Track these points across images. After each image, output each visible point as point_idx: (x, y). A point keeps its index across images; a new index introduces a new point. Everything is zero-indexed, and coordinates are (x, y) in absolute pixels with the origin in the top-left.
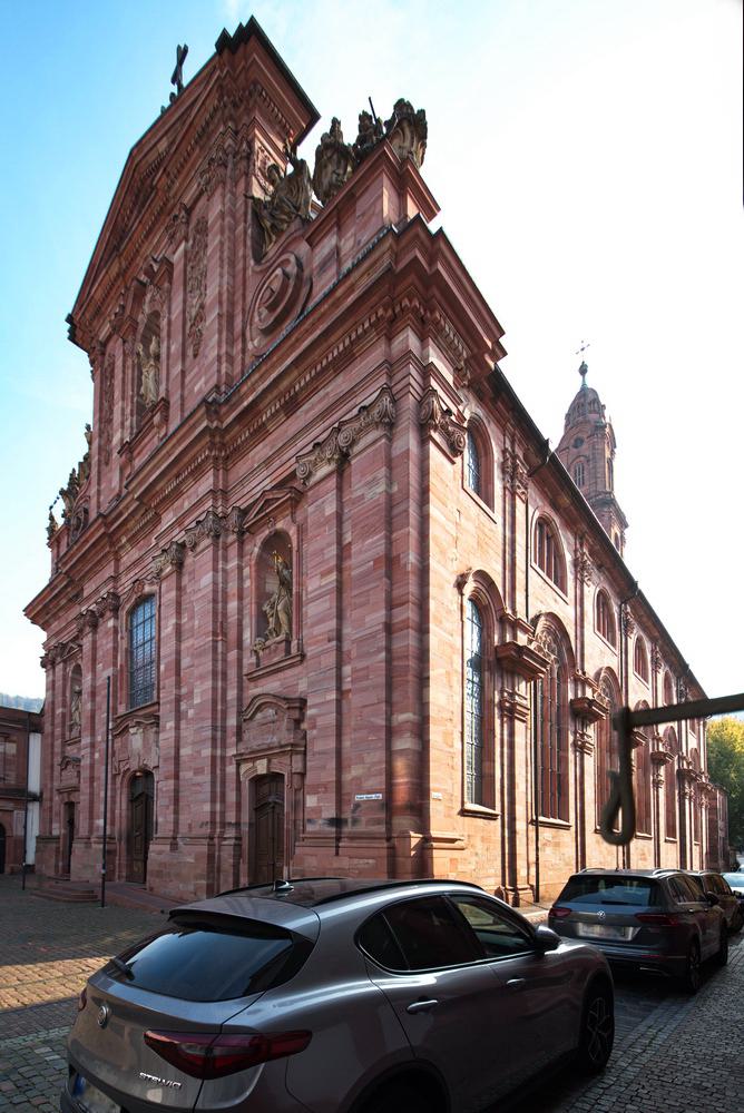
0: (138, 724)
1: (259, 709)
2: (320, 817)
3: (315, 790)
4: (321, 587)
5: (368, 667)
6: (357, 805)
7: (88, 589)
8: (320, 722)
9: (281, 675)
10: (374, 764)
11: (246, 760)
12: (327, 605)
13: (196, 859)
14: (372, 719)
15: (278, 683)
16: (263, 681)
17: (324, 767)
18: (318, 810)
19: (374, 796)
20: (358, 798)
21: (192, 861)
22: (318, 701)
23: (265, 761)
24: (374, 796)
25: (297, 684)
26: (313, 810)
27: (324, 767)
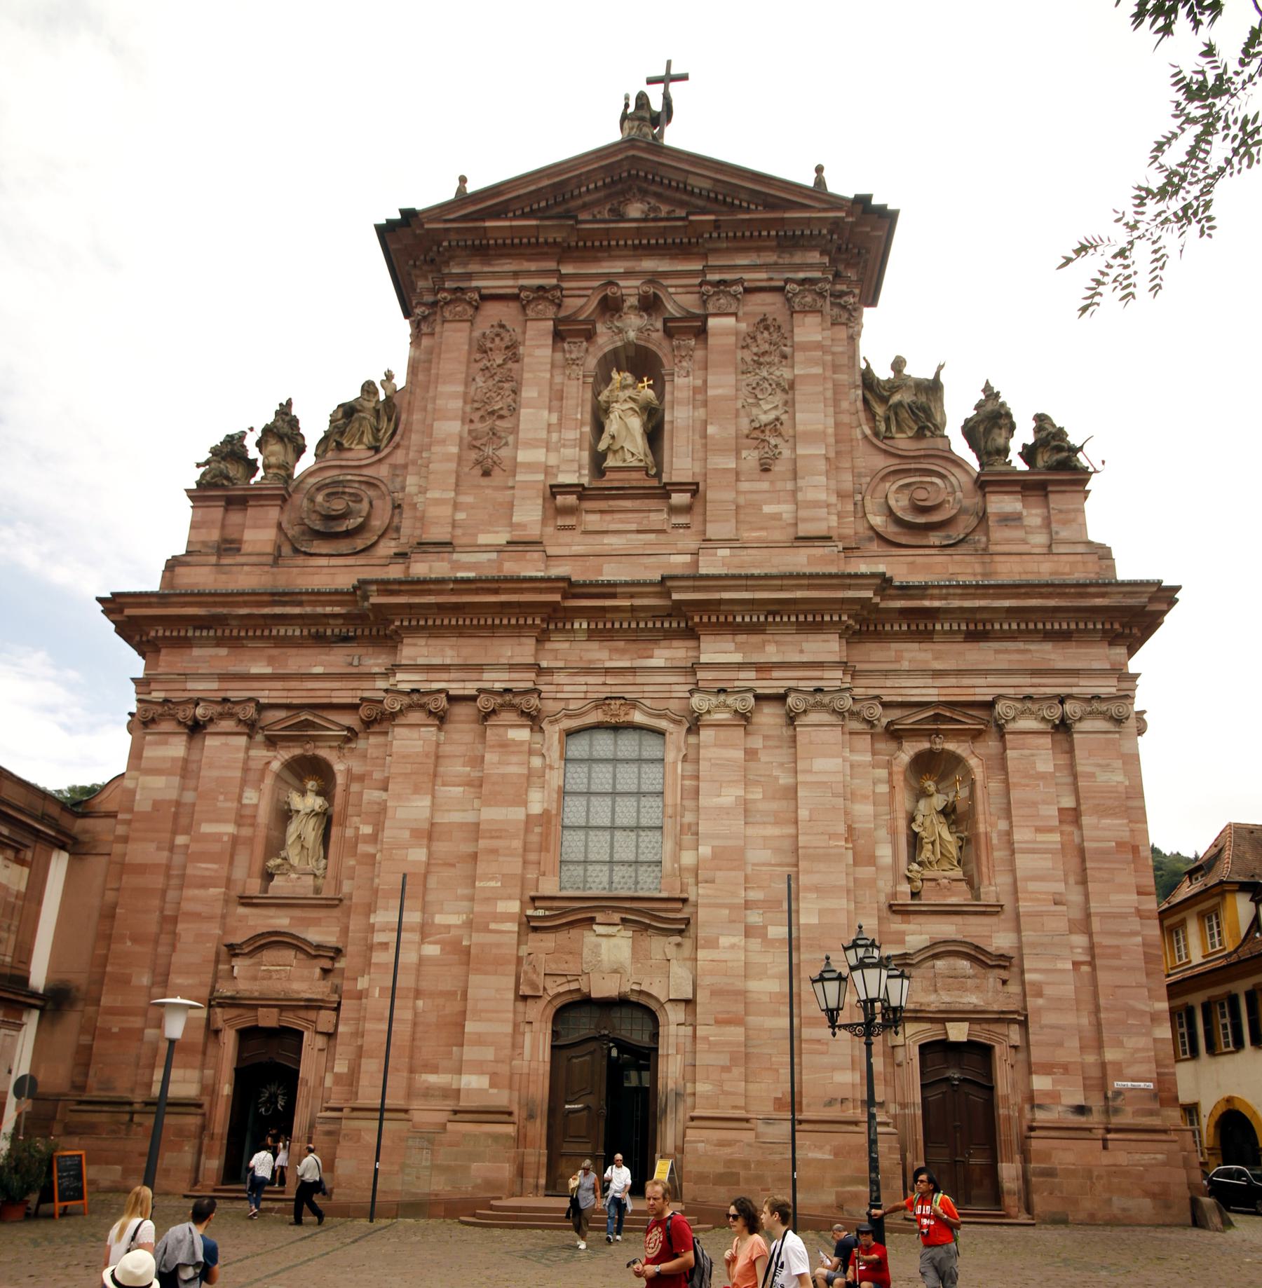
0: (624, 920)
1: (936, 956)
2: (1059, 1104)
3: (1047, 1069)
4: (1035, 842)
5: (1118, 947)
6: (1118, 1093)
7: (415, 650)
8: (1048, 991)
9: (958, 919)
10: (1137, 1050)
11: (917, 1020)
12: (1049, 864)
13: (836, 1155)
14: (1132, 1002)
15: (954, 928)
16: (921, 919)
17: (1060, 1045)
18: (1054, 1096)
19: (1142, 1085)
20: (1118, 1084)
21: (832, 1157)
22: (1042, 965)
23: (966, 1025)
24: (1142, 1085)
25: (991, 937)
26: (1047, 1094)
27: (1060, 1045)
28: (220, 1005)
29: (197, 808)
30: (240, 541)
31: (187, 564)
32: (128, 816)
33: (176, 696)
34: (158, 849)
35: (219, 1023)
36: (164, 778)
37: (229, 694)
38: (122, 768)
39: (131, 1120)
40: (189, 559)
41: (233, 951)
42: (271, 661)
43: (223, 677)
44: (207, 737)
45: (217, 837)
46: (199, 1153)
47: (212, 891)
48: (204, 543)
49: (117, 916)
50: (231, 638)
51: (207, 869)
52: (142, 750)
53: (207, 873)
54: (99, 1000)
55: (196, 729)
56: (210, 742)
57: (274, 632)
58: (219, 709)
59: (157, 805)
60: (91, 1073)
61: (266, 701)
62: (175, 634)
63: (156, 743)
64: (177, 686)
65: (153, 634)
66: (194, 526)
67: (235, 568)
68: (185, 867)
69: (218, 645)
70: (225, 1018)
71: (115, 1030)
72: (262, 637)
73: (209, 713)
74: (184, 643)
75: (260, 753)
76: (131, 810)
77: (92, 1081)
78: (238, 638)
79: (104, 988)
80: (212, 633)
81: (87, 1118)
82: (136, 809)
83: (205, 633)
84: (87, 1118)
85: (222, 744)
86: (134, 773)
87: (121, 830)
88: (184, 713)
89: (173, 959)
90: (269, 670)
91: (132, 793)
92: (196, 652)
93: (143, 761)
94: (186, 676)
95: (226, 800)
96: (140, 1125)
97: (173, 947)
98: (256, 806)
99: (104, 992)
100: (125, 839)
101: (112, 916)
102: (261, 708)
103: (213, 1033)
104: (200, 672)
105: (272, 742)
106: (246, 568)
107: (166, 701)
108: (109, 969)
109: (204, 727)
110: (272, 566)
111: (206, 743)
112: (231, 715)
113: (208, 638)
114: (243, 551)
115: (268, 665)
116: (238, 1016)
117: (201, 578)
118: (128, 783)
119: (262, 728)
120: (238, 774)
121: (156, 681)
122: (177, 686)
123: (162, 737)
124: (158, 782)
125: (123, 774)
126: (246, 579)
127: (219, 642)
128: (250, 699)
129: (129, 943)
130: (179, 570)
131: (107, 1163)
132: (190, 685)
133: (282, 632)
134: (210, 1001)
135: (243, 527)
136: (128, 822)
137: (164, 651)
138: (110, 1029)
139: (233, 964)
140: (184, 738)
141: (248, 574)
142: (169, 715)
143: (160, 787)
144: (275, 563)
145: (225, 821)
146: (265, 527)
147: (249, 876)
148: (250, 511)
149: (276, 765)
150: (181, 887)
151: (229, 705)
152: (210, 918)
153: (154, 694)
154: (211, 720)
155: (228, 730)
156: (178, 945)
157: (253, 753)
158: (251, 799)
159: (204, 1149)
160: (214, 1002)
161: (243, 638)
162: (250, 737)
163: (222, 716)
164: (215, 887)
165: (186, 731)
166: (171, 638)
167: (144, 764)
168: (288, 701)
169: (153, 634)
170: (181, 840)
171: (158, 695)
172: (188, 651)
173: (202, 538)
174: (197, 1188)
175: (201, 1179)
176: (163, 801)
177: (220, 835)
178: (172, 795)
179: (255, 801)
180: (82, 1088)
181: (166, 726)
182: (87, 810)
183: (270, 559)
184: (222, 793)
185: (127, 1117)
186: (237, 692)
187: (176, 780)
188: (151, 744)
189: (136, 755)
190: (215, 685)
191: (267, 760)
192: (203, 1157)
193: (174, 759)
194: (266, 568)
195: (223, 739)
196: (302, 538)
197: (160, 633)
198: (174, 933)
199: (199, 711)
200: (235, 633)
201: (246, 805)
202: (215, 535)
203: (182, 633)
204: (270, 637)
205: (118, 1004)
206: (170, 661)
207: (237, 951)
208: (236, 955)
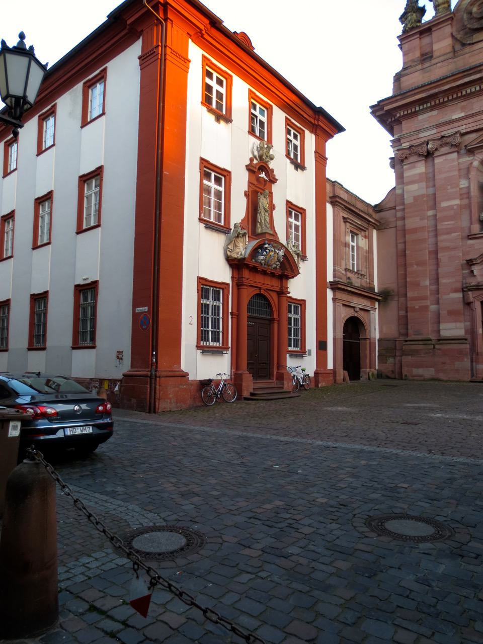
28: (470, 290)
29: (437, 195)
30: (432, 52)
31: (407, 75)
32: (401, 207)
33: (415, 143)
34: (421, 219)
35: (471, 299)
36: (416, 185)
37: (443, 133)
38: (393, 184)
39: (434, 348)
40: (406, 72)
41: (470, 263)
42: (463, 109)
43: (438, 126)
44: (435, 159)
45: (450, 208)
46: (472, 361)
47: (454, 235)
48: (413, 61)
49: (407, 255)
50: (440, 104)
51: (448, 224)
52: (402, 174)
53: (448, 227)
54: (406, 294)
55: (429, 155)
56: (437, 161)
57: (464, 93)
58: (439, 143)
59: (416, 198)
60: (409, 327)
61: (464, 131)
62: (409, 111)
63: (410, 169)
64: (415, 137)
65: (398, 115)
66: (404, 55)
67: (432, 67)
68: (436, 226)
69: (432, 110)
70: (474, 296)
71: (417, 307)
72: (457, 98)
73: (435, 147)
74: (415, 114)
75: (466, 159)
76: (403, 204)
77: (410, 331)
78: (444, 102)
79: (408, 289)
80: (429, 105)
81: (413, 347)
82: (405, 203)
83: (425, 106)
84: (413, 347)
85: (444, 160)
86: (400, 186)
87: (399, 214)
88: (423, 150)
89: (439, 271)
90: (463, 115)
91: (403, 195)
92: (420, 117)
93: (405, 179)
94: (418, 131)
95: (452, 188)
96: (439, 349)
97: (438, 265)
98: (469, 187)
99: (408, 291)
100: (403, 218)
101: (405, 255)
102: (462, 135)
103: (468, 304)
104: (425, 127)
105: (471, 151)
106: (438, 65)
107: (411, 146)
108: (408, 280)
109: (433, 154)
110: (453, 58)
111: (435, 162)
112: (447, 144)
113: (427, 108)
114: (434, 57)
115: (462, 112)
116: (481, 294)
117: (416, 79)
118: (398, 192)
119: (466, 146)
120: (456, 173)
121: (403, 138)
122: (415, 137)
123: (413, 164)
124: (414, 187)
125: (395, 187)
126: (439, 70)
127: (432, 108)
128: (457, 133)
129: (415, 267)
130: (403, 79)
131: (426, 367)
132: (421, 135)
133: (469, 91)
134: (463, 289)
135: (431, 44)
136: (404, 210)
137: (403, 123)
138: (414, 307)
139: (472, 269)
140: (423, 162)
141: (440, 67)
142: (414, 153)
143: (414, 190)
144: (454, 57)
145: (454, 198)
146: (445, 39)
147: (471, 224)
148: (434, 34)
149: (476, 163)
150: (436, 236)
151: (445, 139)
152: (455, 248)
153: (403, 145)
154: (436, 149)
155: (446, 152)
156: (441, 264)
157: (461, 160)
158: (464, 184)
159: (474, 359)
160: (465, 290)
161: (446, 102)
162: (458, 152)
163: (442, 146)
164: (455, 233)
165: (424, 158)
166: (408, 114)
167: (405, 180)
168: (477, 127)
169: (398, 115)
170: (430, 213)
171: (406, 145)
172: (415, 119)
173: (410, 59)
174: (474, 378)
175: (475, 374)
176: (419, 196)
177: (452, 206)
178: (424, 192)
179: (467, 185)
180: (407, 335)
181: (412, 159)
182: (380, 209)
183: (451, 55)
184: (448, 185)
185: (432, 346)
186: (448, 131)
187: (424, 184)
188: (406, 170)
189: (400, 178)
190: (434, 131)
191: (469, 162)
192: (474, 364)
193: (420, 174)
194: (450, 61)
195: (444, 157)
196: (466, 37)
197: (402, 114)
198: (437, 259)
199: (430, 146)
200: (442, 100)
201: (462, 188)
202: (417, 54)
203: (413, 110)
204: (462, 96)
205: (416, 295)
206: (407, 126)
207: (474, 262)
208: (474, 264)
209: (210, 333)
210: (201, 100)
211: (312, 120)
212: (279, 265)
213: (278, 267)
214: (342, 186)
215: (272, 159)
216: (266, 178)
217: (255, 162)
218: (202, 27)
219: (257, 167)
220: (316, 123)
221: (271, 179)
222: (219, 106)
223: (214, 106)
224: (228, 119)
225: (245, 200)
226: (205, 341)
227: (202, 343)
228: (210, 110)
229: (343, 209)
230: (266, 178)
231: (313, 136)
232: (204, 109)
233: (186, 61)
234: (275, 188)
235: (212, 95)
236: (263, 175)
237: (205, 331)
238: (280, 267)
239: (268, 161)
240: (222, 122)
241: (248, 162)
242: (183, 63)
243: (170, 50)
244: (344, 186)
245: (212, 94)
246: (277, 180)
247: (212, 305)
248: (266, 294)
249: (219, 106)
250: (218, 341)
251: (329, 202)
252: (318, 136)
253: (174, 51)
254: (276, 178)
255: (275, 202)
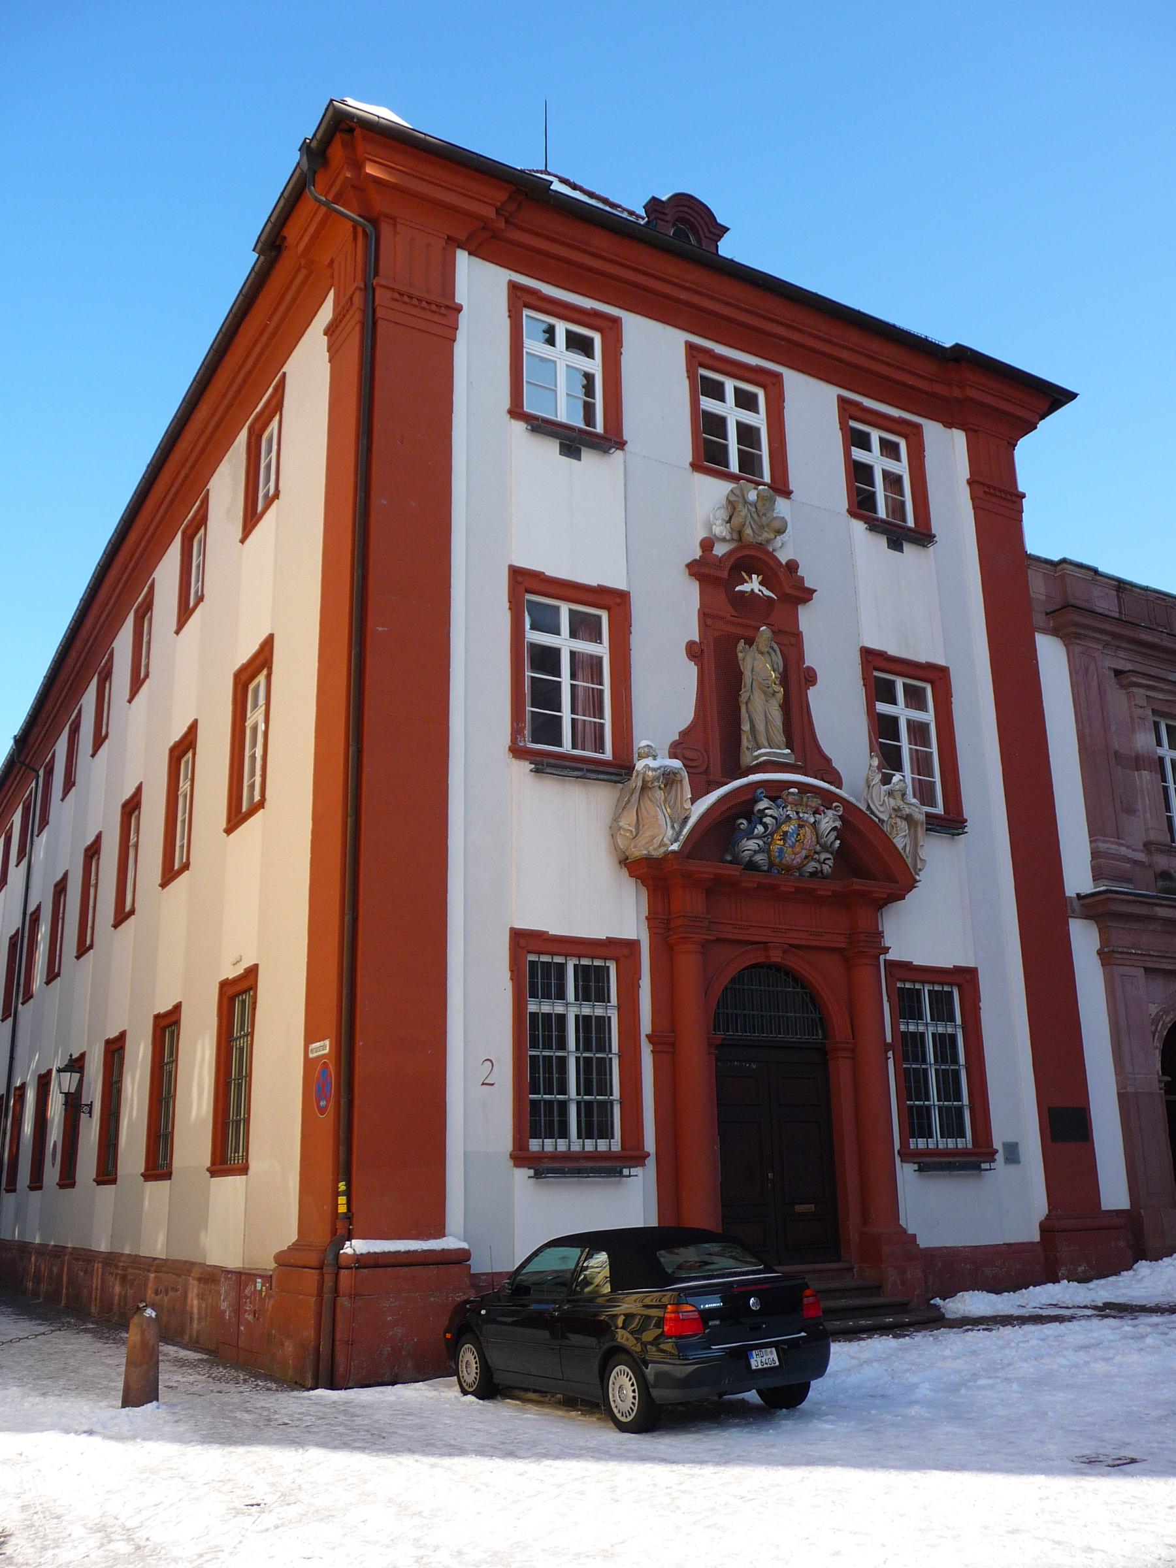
209: (573, 1110)
210: (690, 459)
211: (939, 389)
212: (830, 863)
213: (826, 868)
214: (1095, 571)
215: (780, 531)
216: (767, 593)
217: (720, 550)
218: (490, 213)
219: (729, 564)
220: (957, 393)
221: (788, 591)
222: (897, 508)
223: (882, 513)
224: (923, 536)
225: (690, 672)
226: (551, 1136)
227: (534, 1145)
228: (874, 525)
229: (1106, 645)
230: (767, 593)
231: (959, 438)
232: (859, 526)
233: (443, 310)
234: (808, 619)
235: (760, 450)
236: (753, 585)
237: (550, 1103)
238: (833, 868)
239: (768, 541)
240: (907, 547)
241: (697, 554)
242: (436, 318)
243: (389, 294)
244: (1101, 569)
245: (872, 485)
246: (811, 592)
247: (577, 1017)
248: (794, 962)
249: (897, 508)
250: (606, 1133)
251: (1046, 631)
252: (976, 431)
253: (401, 294)
254: (807, 584)
255: (811, 659)
